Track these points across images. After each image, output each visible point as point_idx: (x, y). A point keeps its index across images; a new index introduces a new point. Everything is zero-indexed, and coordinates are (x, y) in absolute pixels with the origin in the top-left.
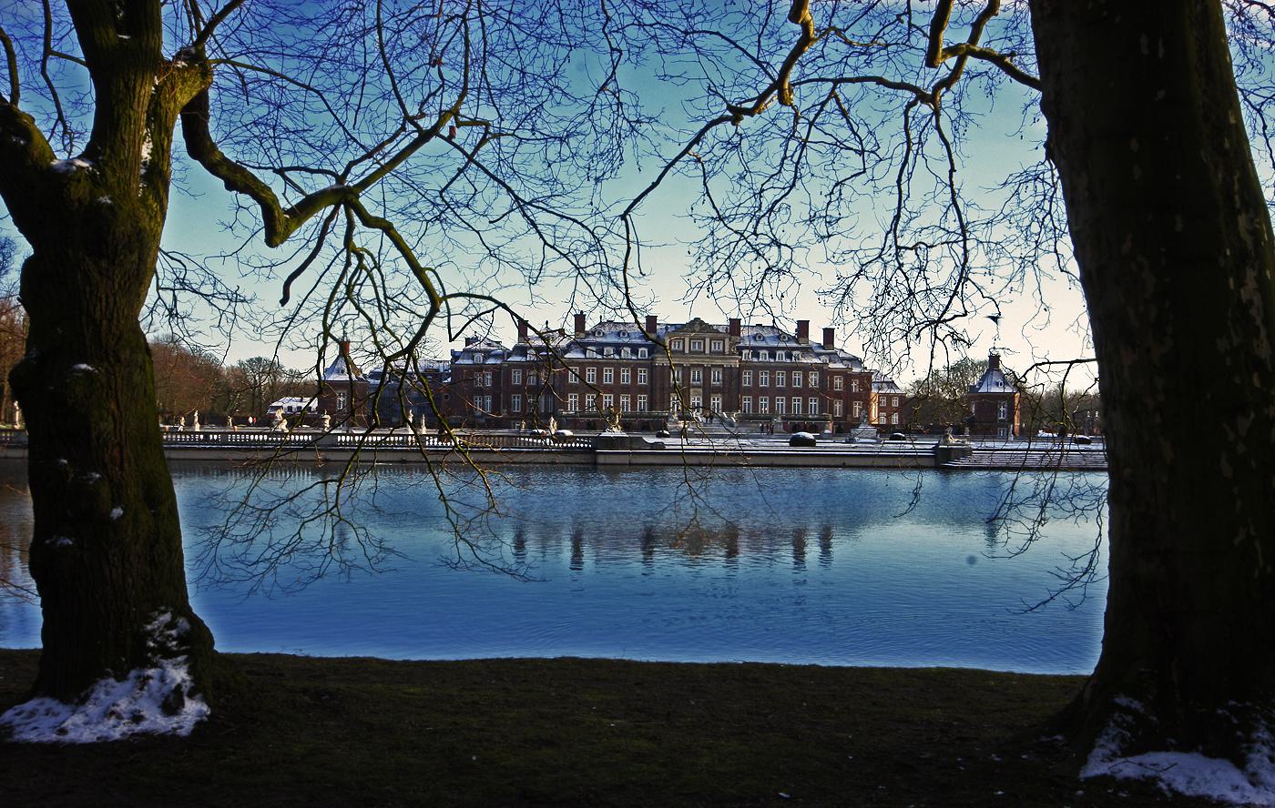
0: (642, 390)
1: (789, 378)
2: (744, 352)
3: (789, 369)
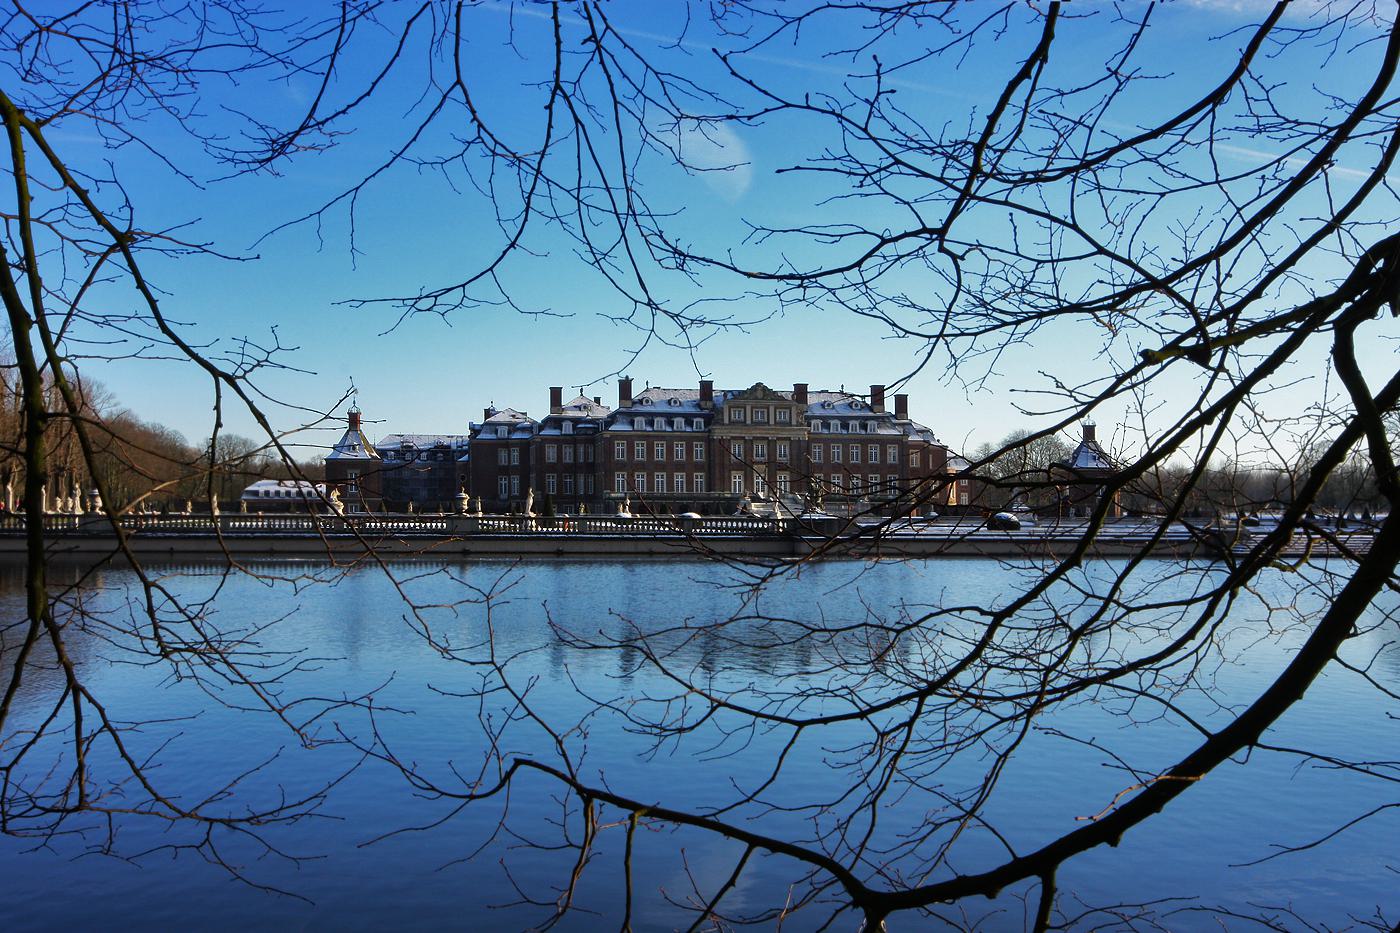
0: (698, 467)
1: (865, 454)
2: (813, 422)
3: (865, 442)
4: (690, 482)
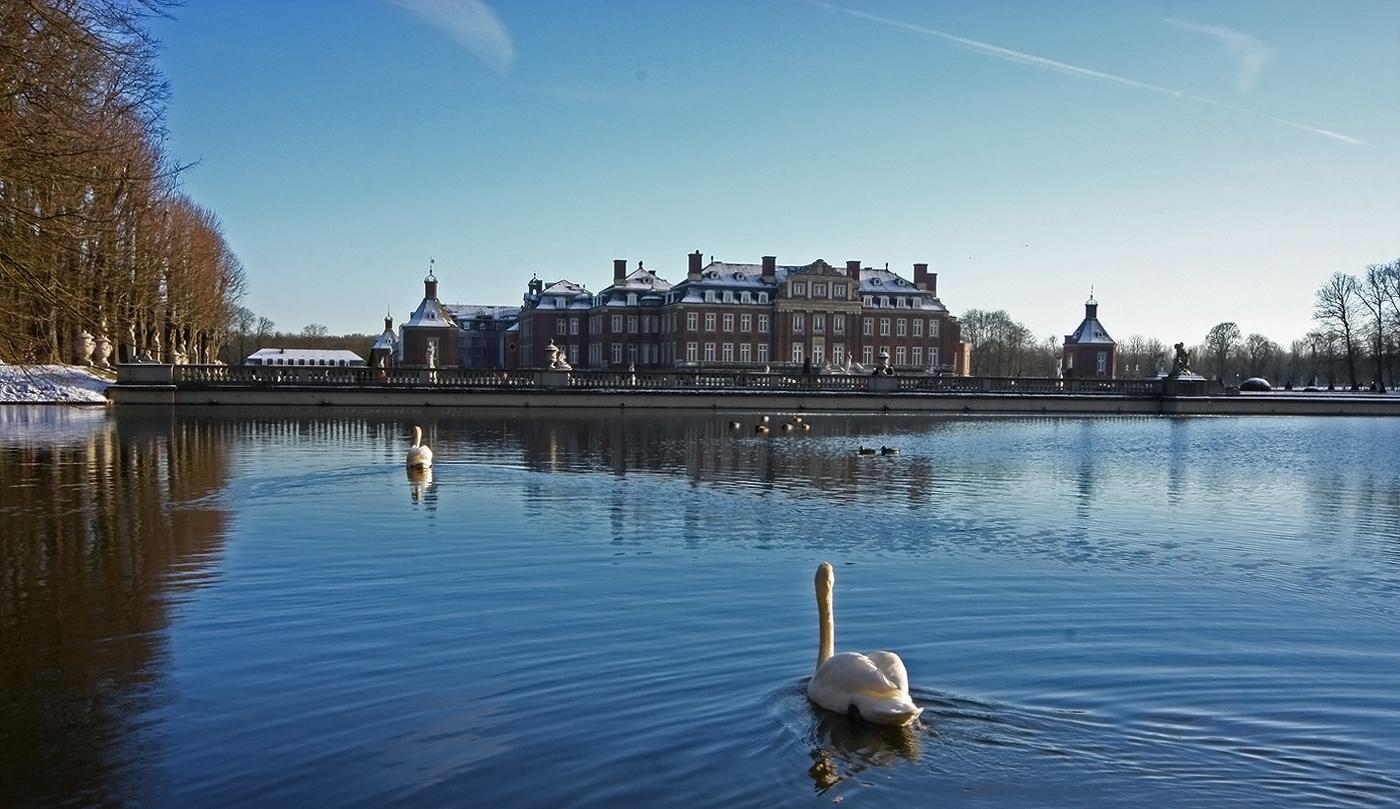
0: (763, 338)
1: (910, 326)
2: (866, 297)
3: (910, 317)
4: (754, 353)
